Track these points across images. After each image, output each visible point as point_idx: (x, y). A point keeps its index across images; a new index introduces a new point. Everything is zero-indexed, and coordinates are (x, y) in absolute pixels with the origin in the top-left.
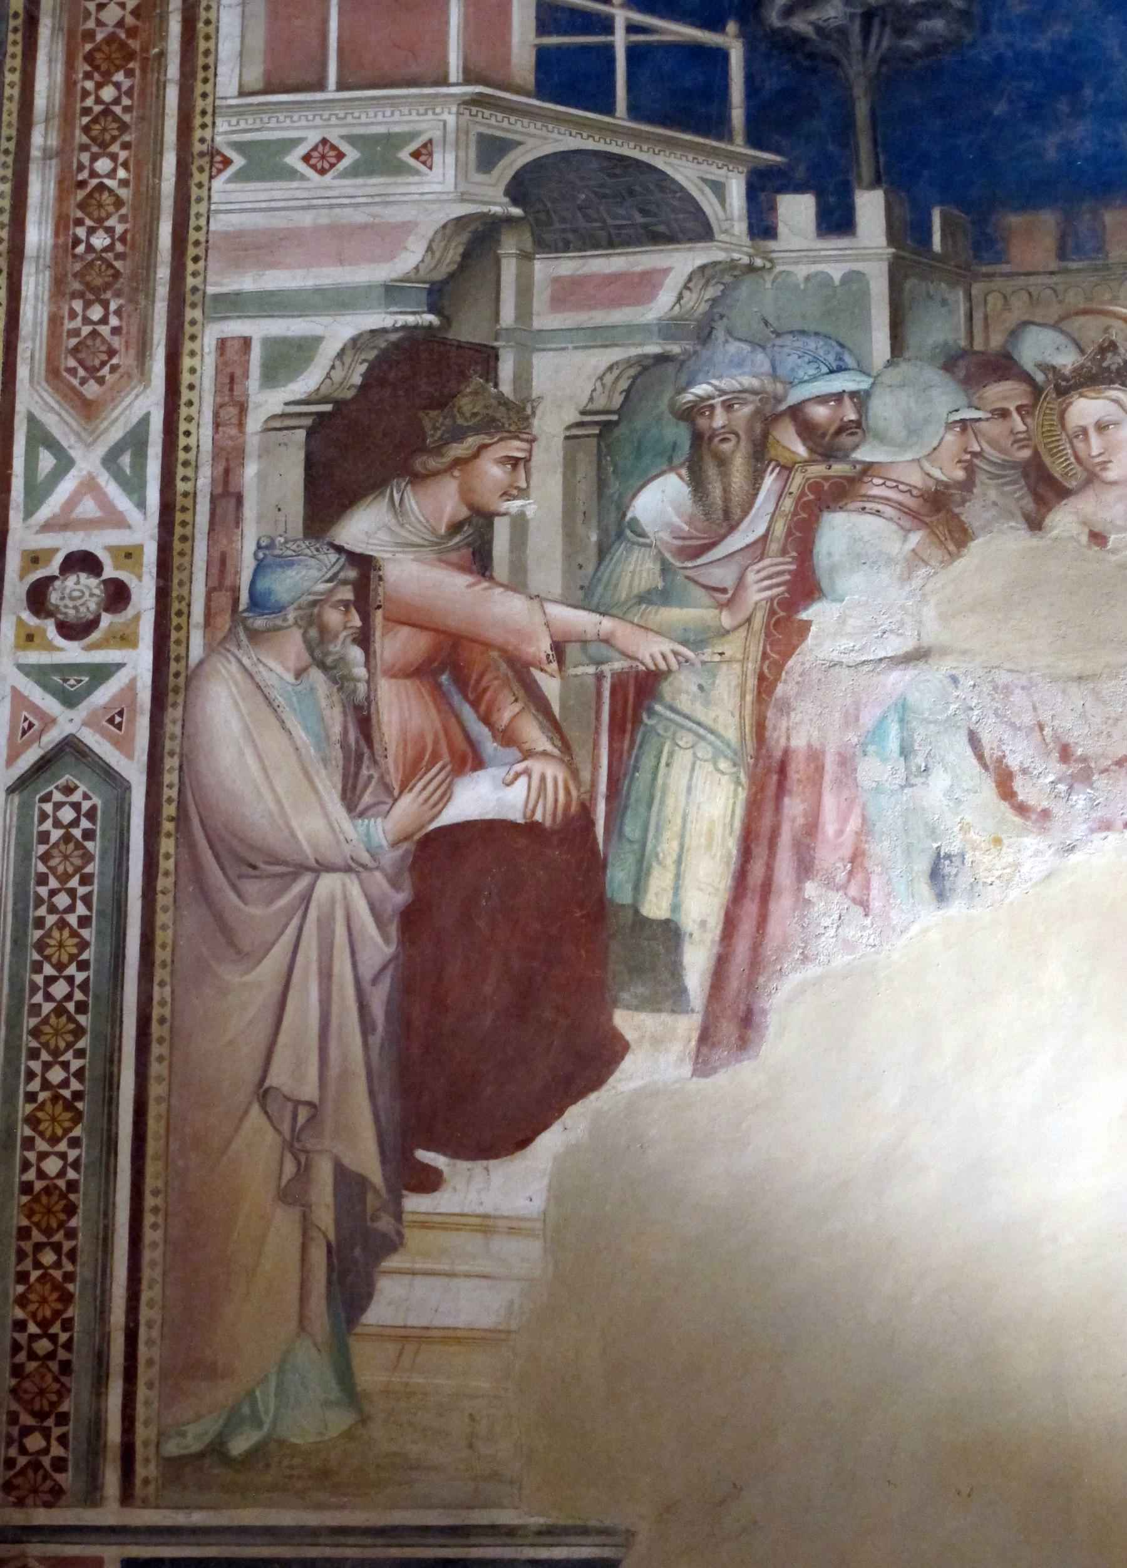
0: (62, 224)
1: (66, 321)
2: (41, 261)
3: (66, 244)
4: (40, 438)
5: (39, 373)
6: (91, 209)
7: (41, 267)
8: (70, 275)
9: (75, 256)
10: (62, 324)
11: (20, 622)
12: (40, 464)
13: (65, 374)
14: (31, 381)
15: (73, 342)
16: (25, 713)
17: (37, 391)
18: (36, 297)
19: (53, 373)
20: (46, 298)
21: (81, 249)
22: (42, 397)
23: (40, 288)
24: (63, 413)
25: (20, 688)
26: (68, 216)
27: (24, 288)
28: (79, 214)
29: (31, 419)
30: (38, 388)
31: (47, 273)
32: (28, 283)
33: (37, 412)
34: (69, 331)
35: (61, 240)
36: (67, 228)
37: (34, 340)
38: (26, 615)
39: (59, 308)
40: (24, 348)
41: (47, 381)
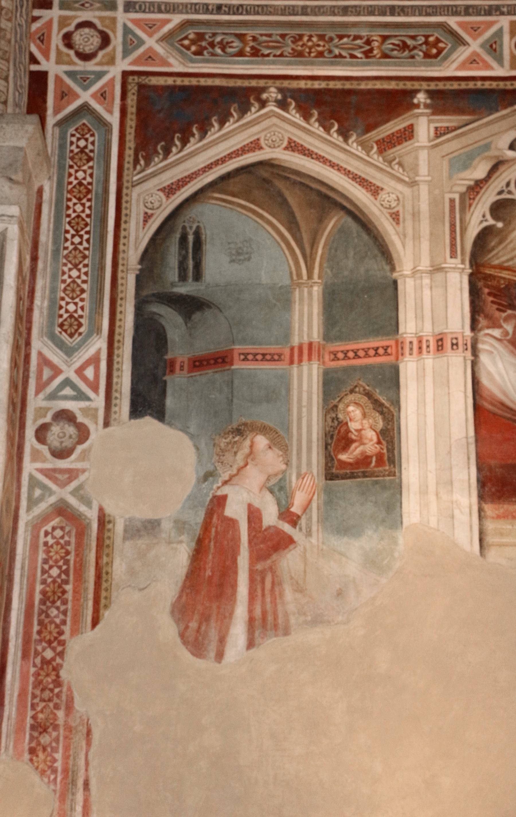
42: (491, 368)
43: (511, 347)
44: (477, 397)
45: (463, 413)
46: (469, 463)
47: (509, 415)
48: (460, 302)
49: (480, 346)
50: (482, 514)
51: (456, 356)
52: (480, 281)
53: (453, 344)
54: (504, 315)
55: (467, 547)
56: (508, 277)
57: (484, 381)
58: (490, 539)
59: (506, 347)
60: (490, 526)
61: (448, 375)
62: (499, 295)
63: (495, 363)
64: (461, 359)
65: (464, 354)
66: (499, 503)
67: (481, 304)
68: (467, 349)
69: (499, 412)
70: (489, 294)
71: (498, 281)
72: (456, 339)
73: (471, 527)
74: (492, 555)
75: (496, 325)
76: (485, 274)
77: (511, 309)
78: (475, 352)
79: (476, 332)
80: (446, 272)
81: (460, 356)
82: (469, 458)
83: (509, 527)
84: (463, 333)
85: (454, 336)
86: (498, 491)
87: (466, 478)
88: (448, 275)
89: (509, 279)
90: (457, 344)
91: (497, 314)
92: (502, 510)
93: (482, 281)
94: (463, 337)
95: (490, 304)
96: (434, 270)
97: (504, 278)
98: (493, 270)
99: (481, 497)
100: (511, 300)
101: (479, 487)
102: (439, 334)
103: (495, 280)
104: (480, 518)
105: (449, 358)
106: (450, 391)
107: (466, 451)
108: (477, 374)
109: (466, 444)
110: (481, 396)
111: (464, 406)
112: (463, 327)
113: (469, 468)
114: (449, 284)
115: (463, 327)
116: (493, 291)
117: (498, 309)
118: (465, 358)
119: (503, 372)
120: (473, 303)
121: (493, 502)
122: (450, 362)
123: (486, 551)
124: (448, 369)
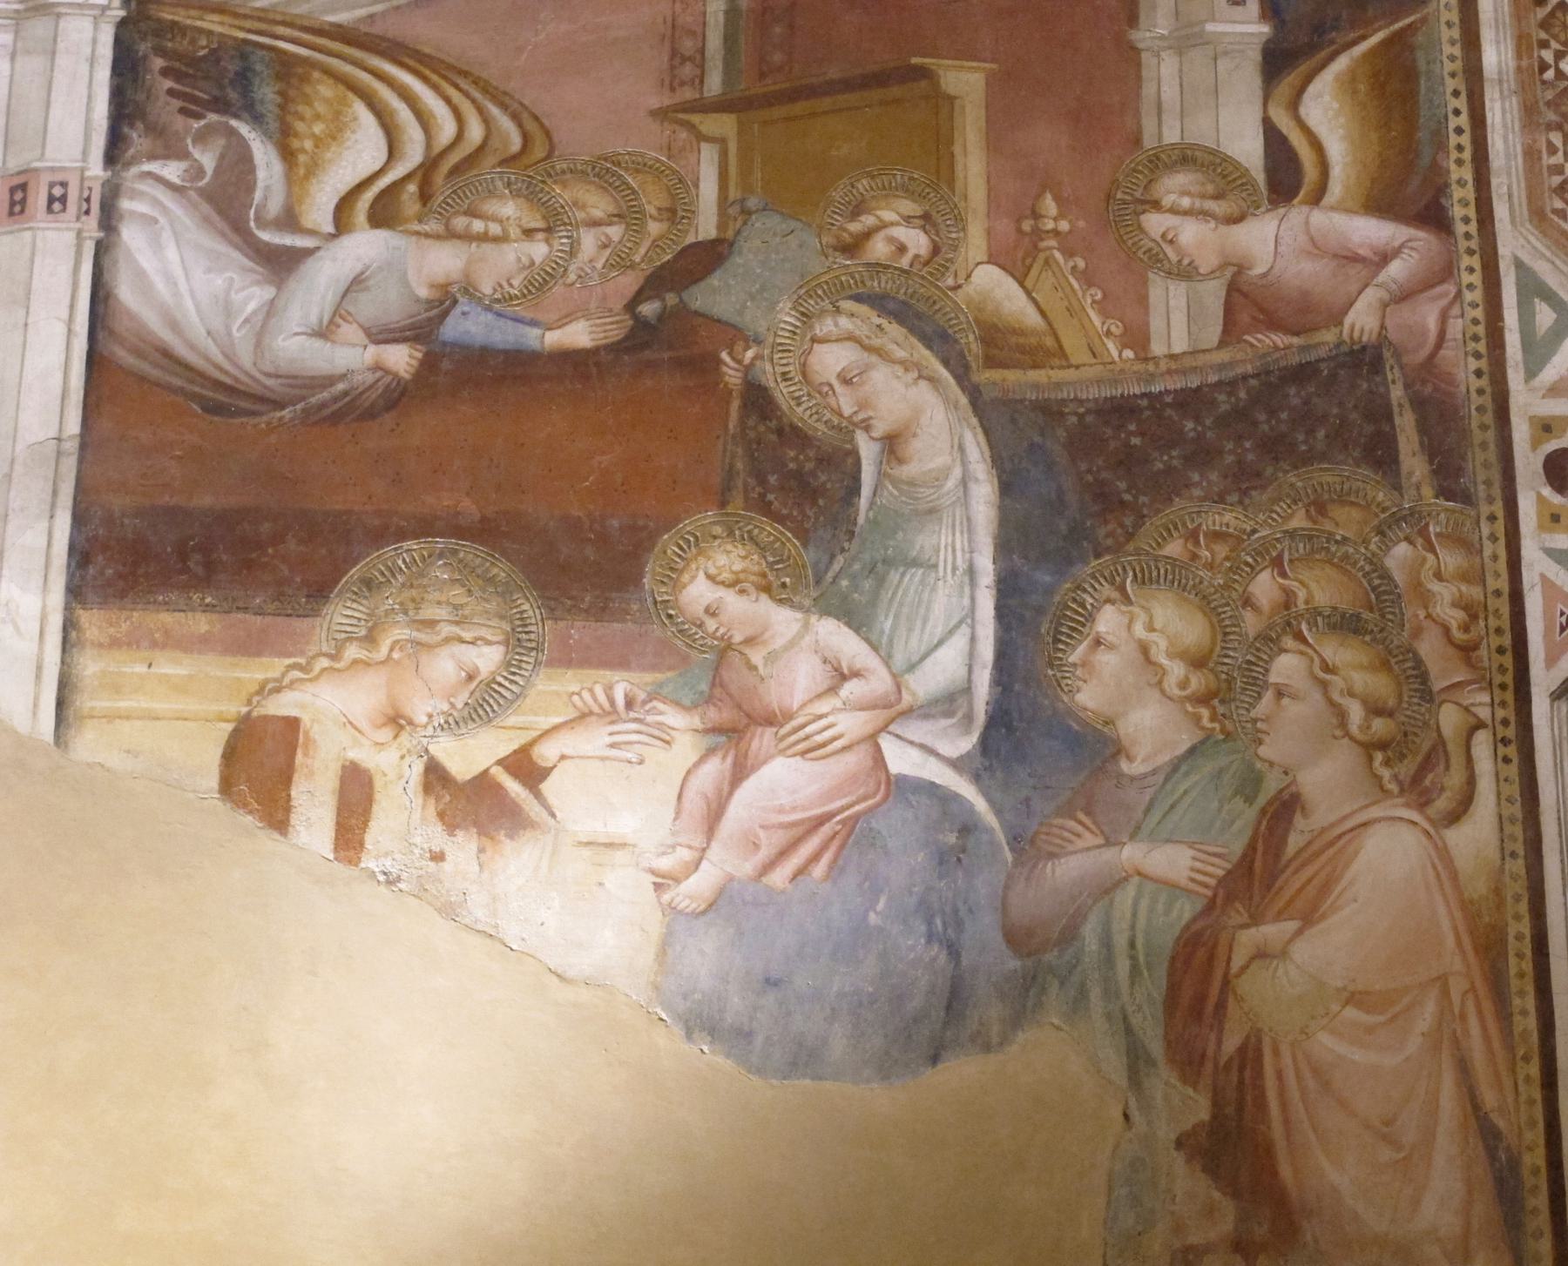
0: (1523, 44)
1: (1545, 155)
2: (1505, 85)
3: (1531, 66)
4: (1532, 288)
5: (1521, 213)
6: (1557, 30)
7: (1506, 93)
8: (1541, 104)
9: (1544, 82)
10: (1540, 159)
11: (1541, 499)
12: (1538, 317)
13: (1552, 216)
14: (1513, 222)
15: (1557, 180)
16: (1560, 606)
17: (1521, 234)
18: (1505, 126)
19: (1538, 215)
20: (1517, 128)
21: (1549, 74)
22: (1529, 242)
23: (1508, 115)
24: (1558, 262)
25: (1551, 576)
26: (1529, 35)
27: (1489, 115)
28: (1543, 35)
29: (1519, 265)
30: (1523, 230)
31: (1514, 99)
32: (1492, 109)
33: (1525, 257)
34: (1549, 167)
35: (1524, 63)
36: (1530, 48)
37: (1509, 174)
38: (1547, 492)
39: (1535, 141)
40: (1499, 184)
41: (1531, 222)
42: (146, 261)
43: (206, 208)
44: (101, 335)
45: (59, 376)
46: (53, 506)
47: (177, 382)
48: (85, 92)
49: (126, 204)
50: (74, 634)
51: (58, 229)
52: (143, 39)
53: (51, 200)
54: (196, 125)
55: (22, 723)
56: (218, 29)
57: (125, 292)
58: (85, 702)
59: (195, 206)
60: (90, 666)
61: (31, 277)
62: (187, 75)
63: (156, 245)
64: (70, 237)
65: (78, 225)
66: (122, 609)
67: (141, 97)
68: (87, 212)
69: (155, 373)
70: (165, 72)
71: (193, 41)
72: (64, 185)
73: (39, 668)
74: (88, 744)
75: (171, 150)
76: (159, 21)
77: (217, 111)
78: (109, 218)
79: (119, 167)
80: (59, 15)
81: (68, 229)
82: (55, 493)
83: (141, 669)
84: (83, 170)
85: (59, 177)
86: (120, 576)
87: (42, 541)
88: (62, 24)
89: (221, 35)
90: (63, 199)
91: (180, 122)
92: (125, 627)
93: (150, 38)
94: (82, 179)
95: (163, 98)
96: (26, 10)
97: (210, 33)
98: (182, 12)
99: (75, 593)
100: (221, 87)
101: (73, 564)
102: (20, 173)
103: (184, 35)
104: (66, 645)
105: (40, 233)
106: (30, 321)
107: (51, 475)
108: (106, 276)
109: (54, 455)
110: (111, 332)
111: (63, 357)
112: (85, 153)
113: (52, 517)
114: (61, 46)
115: (85, 153)
116: (177, 65)
117: (182, 111)
118: (79, 233)
119: (178, 272)
120: (119, 96)
121: (104, 603)
122: (39, 244)
123: (73, 732)
124: (32, 262)
